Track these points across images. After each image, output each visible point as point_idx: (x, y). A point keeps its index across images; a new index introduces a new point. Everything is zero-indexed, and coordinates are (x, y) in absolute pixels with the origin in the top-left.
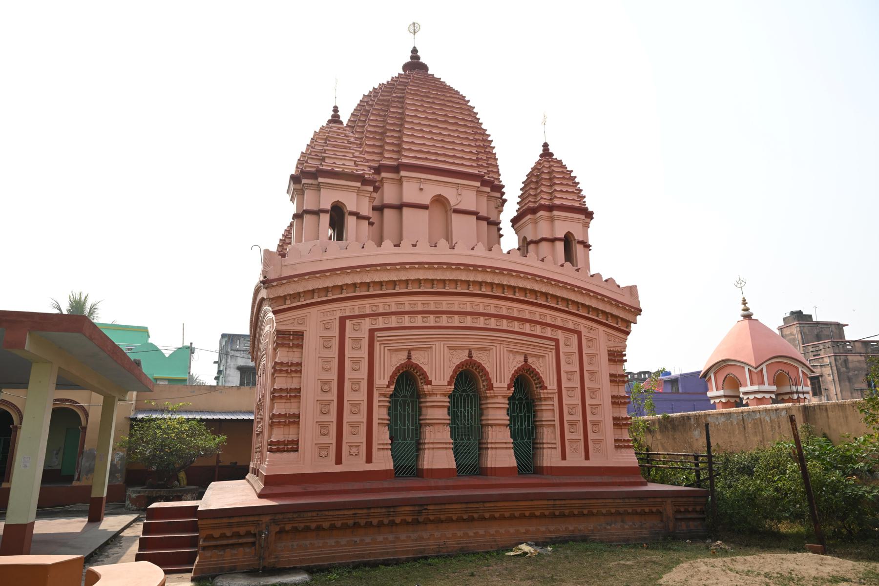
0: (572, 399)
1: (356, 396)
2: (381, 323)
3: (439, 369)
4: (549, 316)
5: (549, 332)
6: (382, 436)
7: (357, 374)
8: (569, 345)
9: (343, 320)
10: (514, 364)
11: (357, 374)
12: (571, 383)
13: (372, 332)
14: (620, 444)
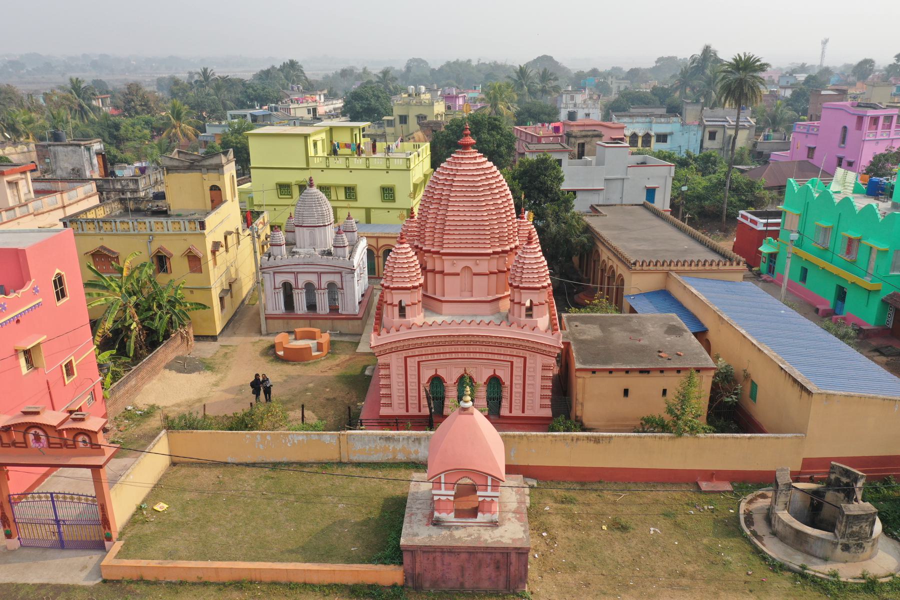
0: (517, 389)
1: (413, 386)
2: (424, 358)
3: (450, 375)
4: (508, 351)
5: (508, 358)
6: (424, 402)
7: (413, 379)
8: (518, 363)
9: (406, 358)
10: (487, 373)
11: (413, 379)
12: (518, 381)
13: (419, 362)
14: (542, 406)
